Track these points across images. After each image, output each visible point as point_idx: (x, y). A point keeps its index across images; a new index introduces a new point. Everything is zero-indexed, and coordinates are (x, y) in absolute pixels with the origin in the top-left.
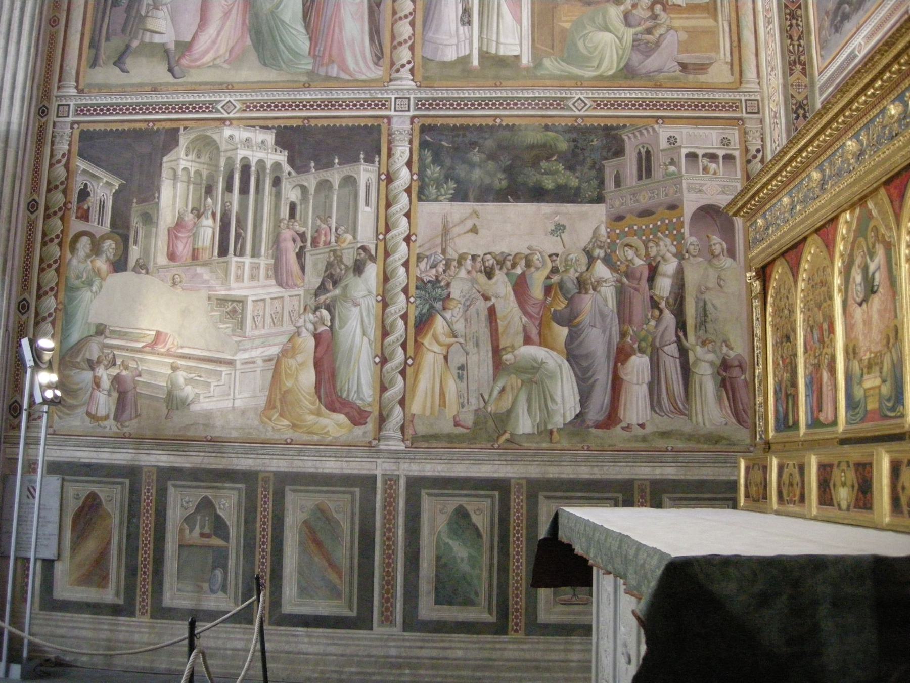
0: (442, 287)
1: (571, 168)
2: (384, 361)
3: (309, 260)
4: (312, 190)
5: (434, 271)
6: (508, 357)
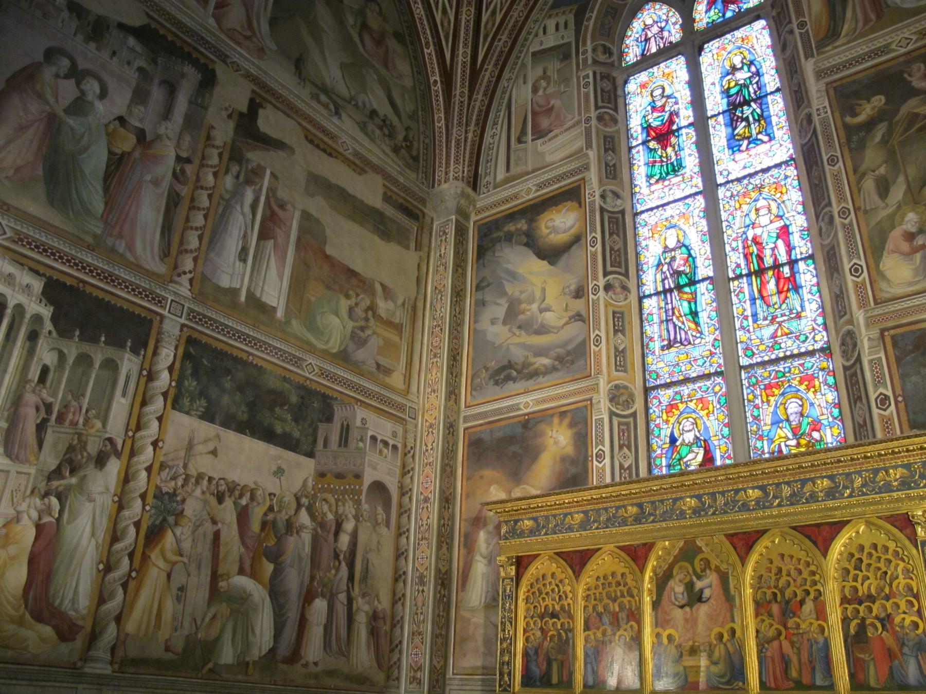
0: (177, 502)
1: (296, 420)
2: (109, 568)
3: (49, 437)
4: (71, 360)
5: (173, 483)
6: (223, 584)
